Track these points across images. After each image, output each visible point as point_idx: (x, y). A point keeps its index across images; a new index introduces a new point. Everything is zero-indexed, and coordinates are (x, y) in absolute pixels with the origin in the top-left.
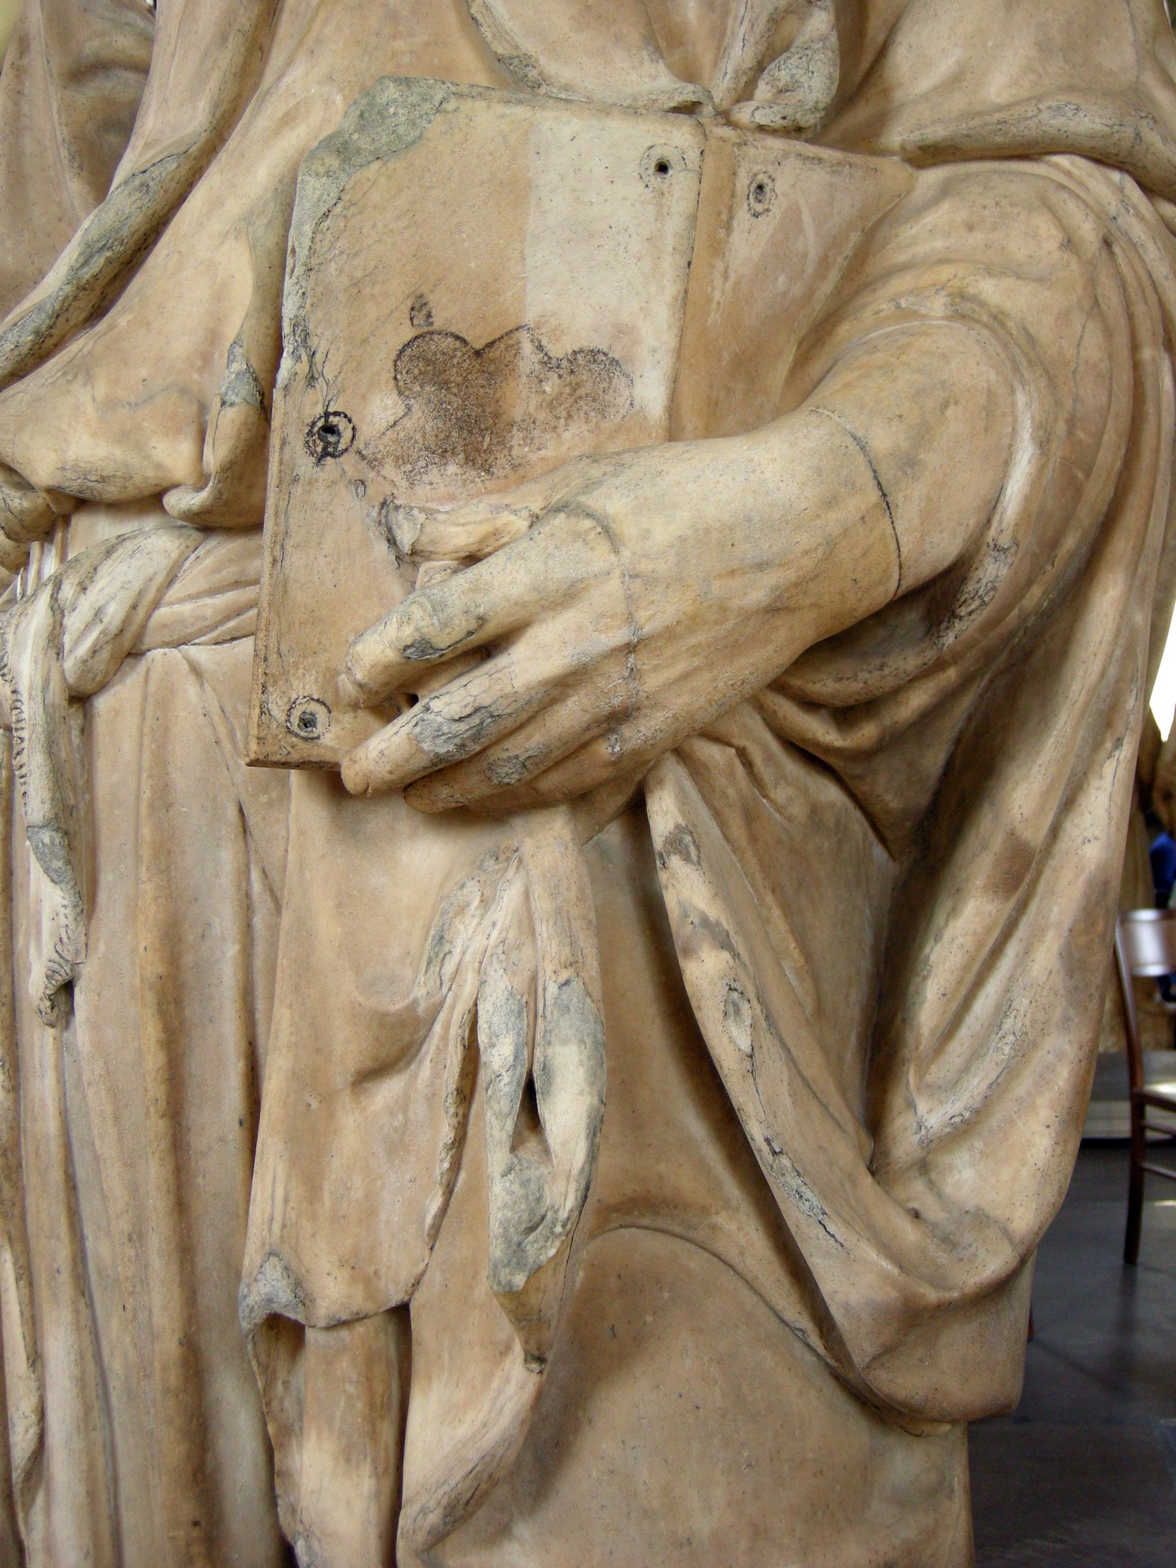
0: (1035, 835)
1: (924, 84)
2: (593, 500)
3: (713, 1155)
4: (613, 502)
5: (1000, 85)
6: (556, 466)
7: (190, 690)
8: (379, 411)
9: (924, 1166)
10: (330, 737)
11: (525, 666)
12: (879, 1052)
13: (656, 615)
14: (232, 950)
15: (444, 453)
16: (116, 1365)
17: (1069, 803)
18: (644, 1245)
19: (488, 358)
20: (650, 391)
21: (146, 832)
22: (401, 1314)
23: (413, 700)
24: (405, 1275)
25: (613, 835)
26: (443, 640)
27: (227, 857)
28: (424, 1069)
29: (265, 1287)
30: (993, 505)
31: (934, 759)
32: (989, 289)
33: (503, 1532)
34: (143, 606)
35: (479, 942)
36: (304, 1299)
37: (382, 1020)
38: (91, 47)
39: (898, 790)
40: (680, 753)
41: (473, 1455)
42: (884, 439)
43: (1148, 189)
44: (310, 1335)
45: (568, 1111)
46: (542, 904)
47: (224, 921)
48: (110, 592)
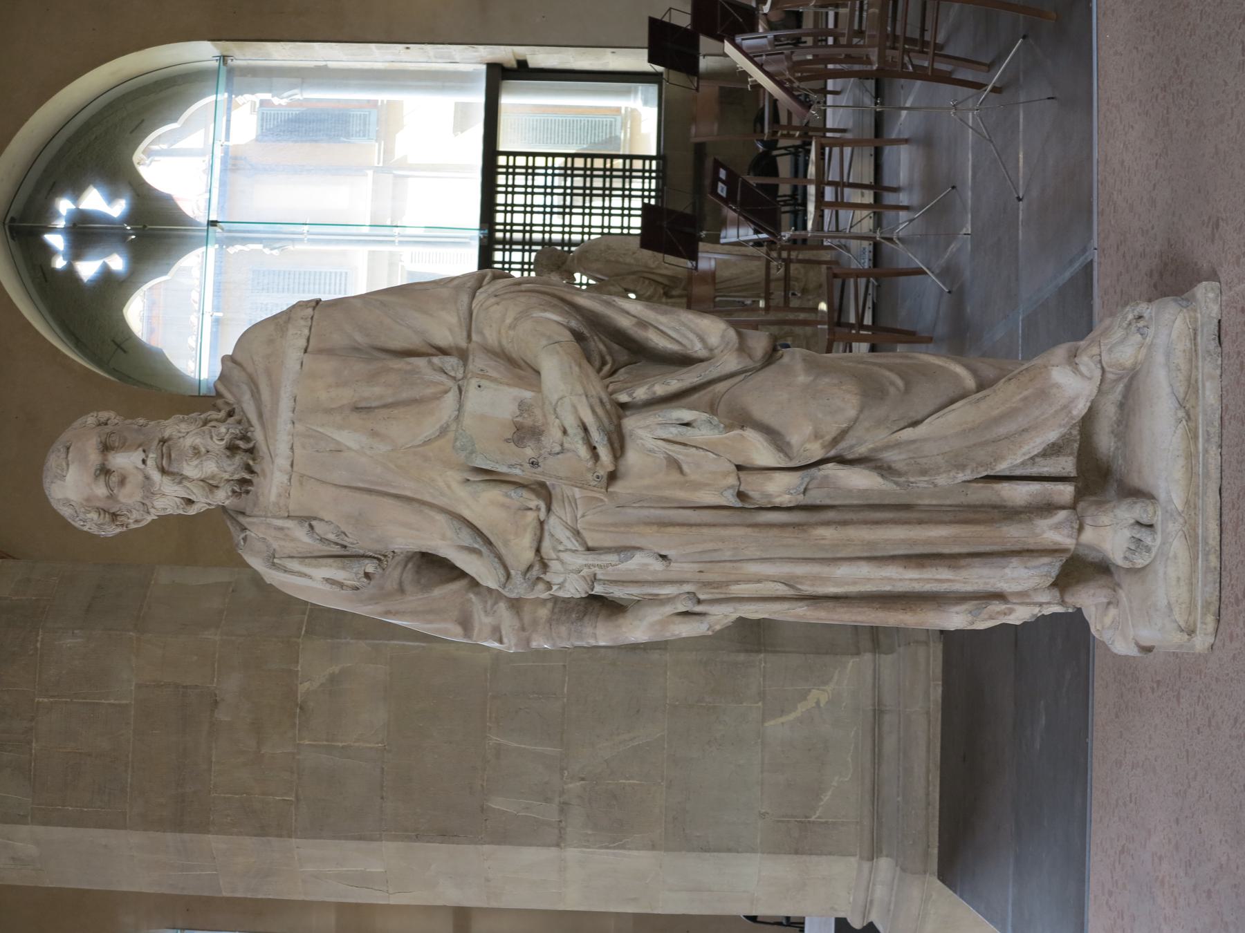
0: (635, 320)
1: (450, 338)
3: (703, 392)
4: (555, 397)
5: (453, 319)
6: (545, 416)
8: (529, 452)
9: (711, 350)
10: (602, 473)
12: (684, 361)
13: (580, 390)
14: (652, 511)
15: (539, 440)
16: (758, 554)
17: (628, 313)
18: (722, 408)
19: (519, 428)
20: (528, 395)
21: (622, 529)
22: (739, 468)
23: (595, 448)
24: (728, 464)
25: (628, 413)
26: (582, 434)
27: (629, 511)
28: (680, 457)
29: (730, 499)
30: (558, 323)
31: (616, 347)
32: (508, 321)
33: (788, 444)
38: (396, 586)
39: (623, 356)
40: (611, 394)
42: (544, 342)
44: (742, 489)
45: (687, 415)
46: (642, 423)
47: (645, 512)
48: (563, 534)
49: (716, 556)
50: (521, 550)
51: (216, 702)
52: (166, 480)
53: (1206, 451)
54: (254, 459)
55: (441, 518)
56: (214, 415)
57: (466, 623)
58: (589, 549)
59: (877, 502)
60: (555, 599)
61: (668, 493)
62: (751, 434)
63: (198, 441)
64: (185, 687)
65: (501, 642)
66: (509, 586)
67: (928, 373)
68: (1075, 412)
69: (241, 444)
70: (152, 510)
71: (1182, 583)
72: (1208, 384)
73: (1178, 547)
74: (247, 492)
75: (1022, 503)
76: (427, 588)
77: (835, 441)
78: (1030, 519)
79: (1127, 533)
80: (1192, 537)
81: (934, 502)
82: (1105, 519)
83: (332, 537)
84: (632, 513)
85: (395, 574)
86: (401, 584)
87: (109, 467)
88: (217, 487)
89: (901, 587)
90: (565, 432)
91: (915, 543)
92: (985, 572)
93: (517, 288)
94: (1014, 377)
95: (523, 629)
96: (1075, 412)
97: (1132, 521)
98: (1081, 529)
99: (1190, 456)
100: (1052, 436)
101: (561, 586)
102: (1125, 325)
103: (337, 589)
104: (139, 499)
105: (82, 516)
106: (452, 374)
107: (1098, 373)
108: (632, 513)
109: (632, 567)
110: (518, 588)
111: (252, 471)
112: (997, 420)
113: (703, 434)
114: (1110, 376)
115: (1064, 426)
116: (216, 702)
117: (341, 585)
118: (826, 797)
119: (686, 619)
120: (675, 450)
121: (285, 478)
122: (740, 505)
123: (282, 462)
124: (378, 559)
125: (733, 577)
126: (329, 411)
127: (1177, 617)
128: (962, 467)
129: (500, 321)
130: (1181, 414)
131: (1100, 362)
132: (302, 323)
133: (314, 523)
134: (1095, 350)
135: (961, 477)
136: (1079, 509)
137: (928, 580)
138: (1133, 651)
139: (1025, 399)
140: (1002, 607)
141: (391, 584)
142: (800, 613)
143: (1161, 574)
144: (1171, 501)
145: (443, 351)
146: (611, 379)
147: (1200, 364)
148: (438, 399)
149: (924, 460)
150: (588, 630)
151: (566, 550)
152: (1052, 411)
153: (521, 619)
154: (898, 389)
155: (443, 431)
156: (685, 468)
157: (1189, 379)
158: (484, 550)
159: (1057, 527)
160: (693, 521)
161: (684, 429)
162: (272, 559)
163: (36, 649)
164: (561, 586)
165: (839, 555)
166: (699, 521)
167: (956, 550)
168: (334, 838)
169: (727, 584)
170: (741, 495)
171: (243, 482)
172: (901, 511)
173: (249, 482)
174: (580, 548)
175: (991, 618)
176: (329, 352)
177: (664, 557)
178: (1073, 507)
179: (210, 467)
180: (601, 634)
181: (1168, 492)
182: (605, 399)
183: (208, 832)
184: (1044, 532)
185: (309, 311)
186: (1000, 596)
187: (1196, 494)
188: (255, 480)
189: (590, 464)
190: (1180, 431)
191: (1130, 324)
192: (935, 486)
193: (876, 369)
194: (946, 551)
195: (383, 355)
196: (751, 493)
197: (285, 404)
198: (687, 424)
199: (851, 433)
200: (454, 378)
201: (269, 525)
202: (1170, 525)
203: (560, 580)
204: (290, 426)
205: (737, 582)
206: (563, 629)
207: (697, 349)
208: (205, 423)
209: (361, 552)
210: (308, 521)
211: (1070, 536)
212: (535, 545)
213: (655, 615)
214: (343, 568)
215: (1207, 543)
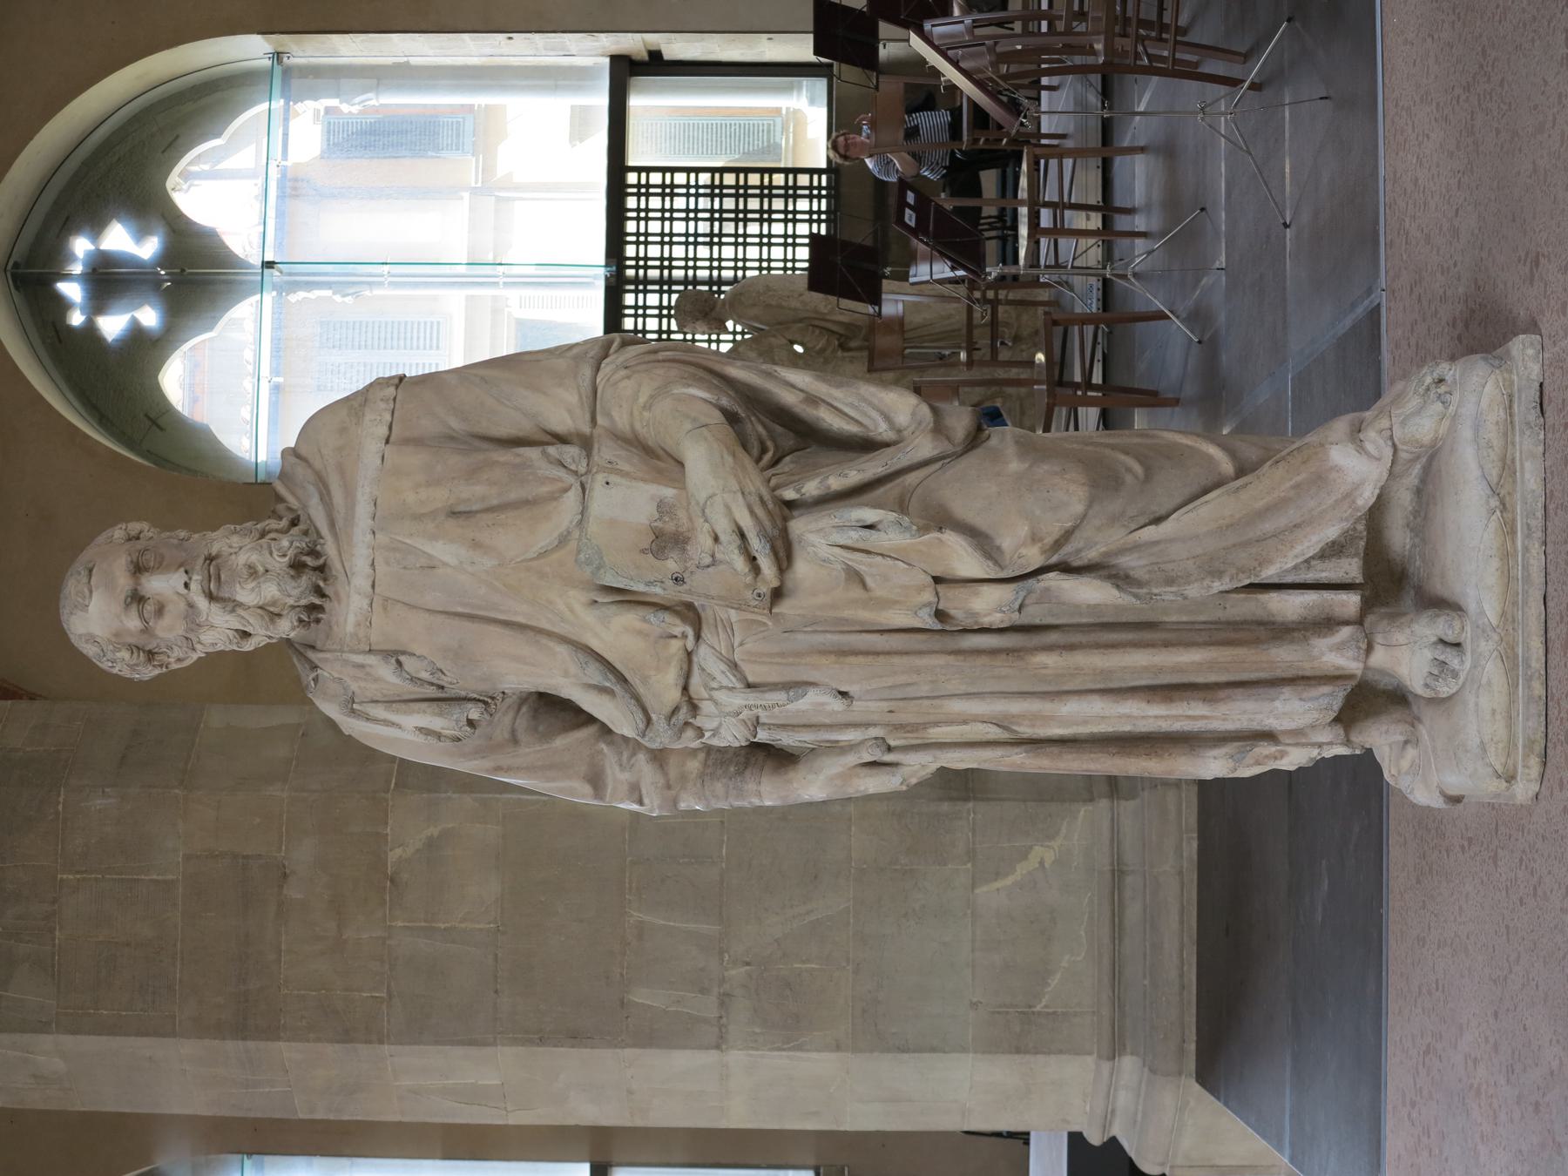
0: (802, 395)
2: (702, 502)
3: (889, 486)
4: (702, 496)
5: (572, 398)
6: (690, 519)
7: (748, 646)
9: (899, 431)
11: (746, 522)
12: (866, 445)
13: (736, 487)
14: (829, 636)
16: (963, 688)
17: (793, 386)
18: (914, 505)
19: (658, 535)
20: (669, 492)
22: (937, 580)
23: (754, 558)
25: (795, 513)
26: (739, 542)
27: (800, 636)
28: (862, 568)
29: (926, 620)
30: (705, 400)
31: (779, 429)
32: (642, 400)
33: (999, 548)
34: (721, 658)
35: (825, 548)
36: (929, 604)
37: (847, 580)
38: (507, 735)
39: (789, 441)
40: (774, 490)
41: (970, 550)
42: (688, 426)
43: (606, 356)
45: (870, 515)
46: (813, 526)
47: (819, 638)
48: (716, 668)
49: (910, 692)
50: (664, 689)
51: (285, 876)
52: (215, 607)
53: (1526, 549)
54: (325, 580)
55: (562, 650)
56: (273, 524)
57: (596, 780)
58: (749, 686)
59: (1111, 620)
60: (709, 749)
61: (847, 613)
62: (951, 538)
63: (254, 558)
64: (245, 857)
65: (641, 803)
66: (650, 734)
67: (1174, 455)
68: (1360, 502)
69: (309, 560)
70: (198, 647)
71: (1498, 717)
72: (1528, 465)
73: (1492, 671)
74: (318, 621)
75: (1295, 617)
76: (547, 737)
77: (1058, 544)
78: (1306, 639)
79: (1428, 654)
80: (1510, 660)
81: (1185, 619)
82: (1400, 637)
83: (425, 675)
84: (803, 640)
85: (505, 720)
86: (513, 732)
87: (143, 593)
88: (279, 615)
89: (1144, 727)
90: (716, 539)
91: (1160, 670)
92: (1250, 706)
93: (652, 357)
94: (1283, 458)
95: (669, 787)
96: (1360, 502)
97: (1434, 639)
98: (1370, 649)
99: (1506, 556)
100: (1332, 532)
101: (715, 732)
102: (1421, 390)
103: (432, 740)
104: (181, 632)
105: (110, 655)
106: (573, 467)
107: (1389, 452)
108: (803, 640)
109: (804, 708)
110: (661, 736)
111: (323, 595)
112: (1262, 514)
113: (893, 538)
114: (1403, 455)
115: (1347, 519)
116: (285, 876)
117: (439, 736)
118: (1054, 981)
119: (875, 771)
120: (857, 561)
121: (365, 603)
122: (939, 627)
123: (361, 582)
124: (485, 702)
125: (932, 718)
126: (418, 517)
127: (1492, 759)
128: (1218, 574)
129: (633, 399)
130: (1494, 502)
131: (1391, 438)
132: (383, 405)
133: (402, 658)
134: (1385, 423)
135: (1217, 586)
136: (1366, 625)
137: (1177, 718)
138: (1437, 803)
139: (1297, 486)
140: (1273, 749)
141: (501, 733)
142: (1018, 760)
143: (1471, 705)
144: (1483, 613)
145: (561, 439)
146: (772, 471)
147: (1517, 439)
148: (556, 499)
149: (1169, 567)
150: (751, 786)
151: (721, 688)
152: (1330, 501)
153: (665, 774)
154: (1136, 477)
155: (563, 540)
156: (869, 580)
157: (1503, 459)
158: (617, 689)
159: (1339, 648)
160: (879, 648)
161: (867, 532)
162: (350, 705)
163: (57, 813)
164: (715, 732)
165: (1066, 688)
166: (887, 648)
167: (1213, 678)
168: (437, 1043)
169: (925, 726)
170: (940, 615)
171: (312, 608)
172: (1141, 630)
173: (320, 608)
174: (738, 685)
175: (1258, 763)
176: (417, 442)
177: (844, 694)
178: (1359, 622)
179: (270, 591)
180: (767, 792)
181: (1479, 602)
182: (767, 497)
183: (279, 1039)
184: (1323, 654)
185: (392, 390)
186: (1269, 736)
187: (1515, 603)
188: (327, 605)
189: (749, 579)
190: (1493, 525)
191: (1428, 389)
192: (1185, 598)
193: (1108, 452)
194: (1200, 679)
195: (485, 445)
196: (952, 612)
197: (363, 510)
198: (871, 527)
199: (1077, 534)
200: (576, 473)
201: (346, 662)
202: (1483, 643)
203: (714, 724)
204: (369, 537)
205: (936, 724)
206: (719, 787)
207: (882, 431)
208: (263, 535)
209: (463, 694)
210: (395, 656)
211: (1356, 659)
212: (681, 682)
213: (834, 766)
214: (441, 715)
215: (1529, 667)
